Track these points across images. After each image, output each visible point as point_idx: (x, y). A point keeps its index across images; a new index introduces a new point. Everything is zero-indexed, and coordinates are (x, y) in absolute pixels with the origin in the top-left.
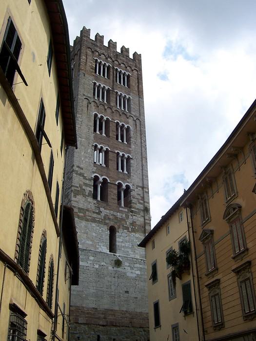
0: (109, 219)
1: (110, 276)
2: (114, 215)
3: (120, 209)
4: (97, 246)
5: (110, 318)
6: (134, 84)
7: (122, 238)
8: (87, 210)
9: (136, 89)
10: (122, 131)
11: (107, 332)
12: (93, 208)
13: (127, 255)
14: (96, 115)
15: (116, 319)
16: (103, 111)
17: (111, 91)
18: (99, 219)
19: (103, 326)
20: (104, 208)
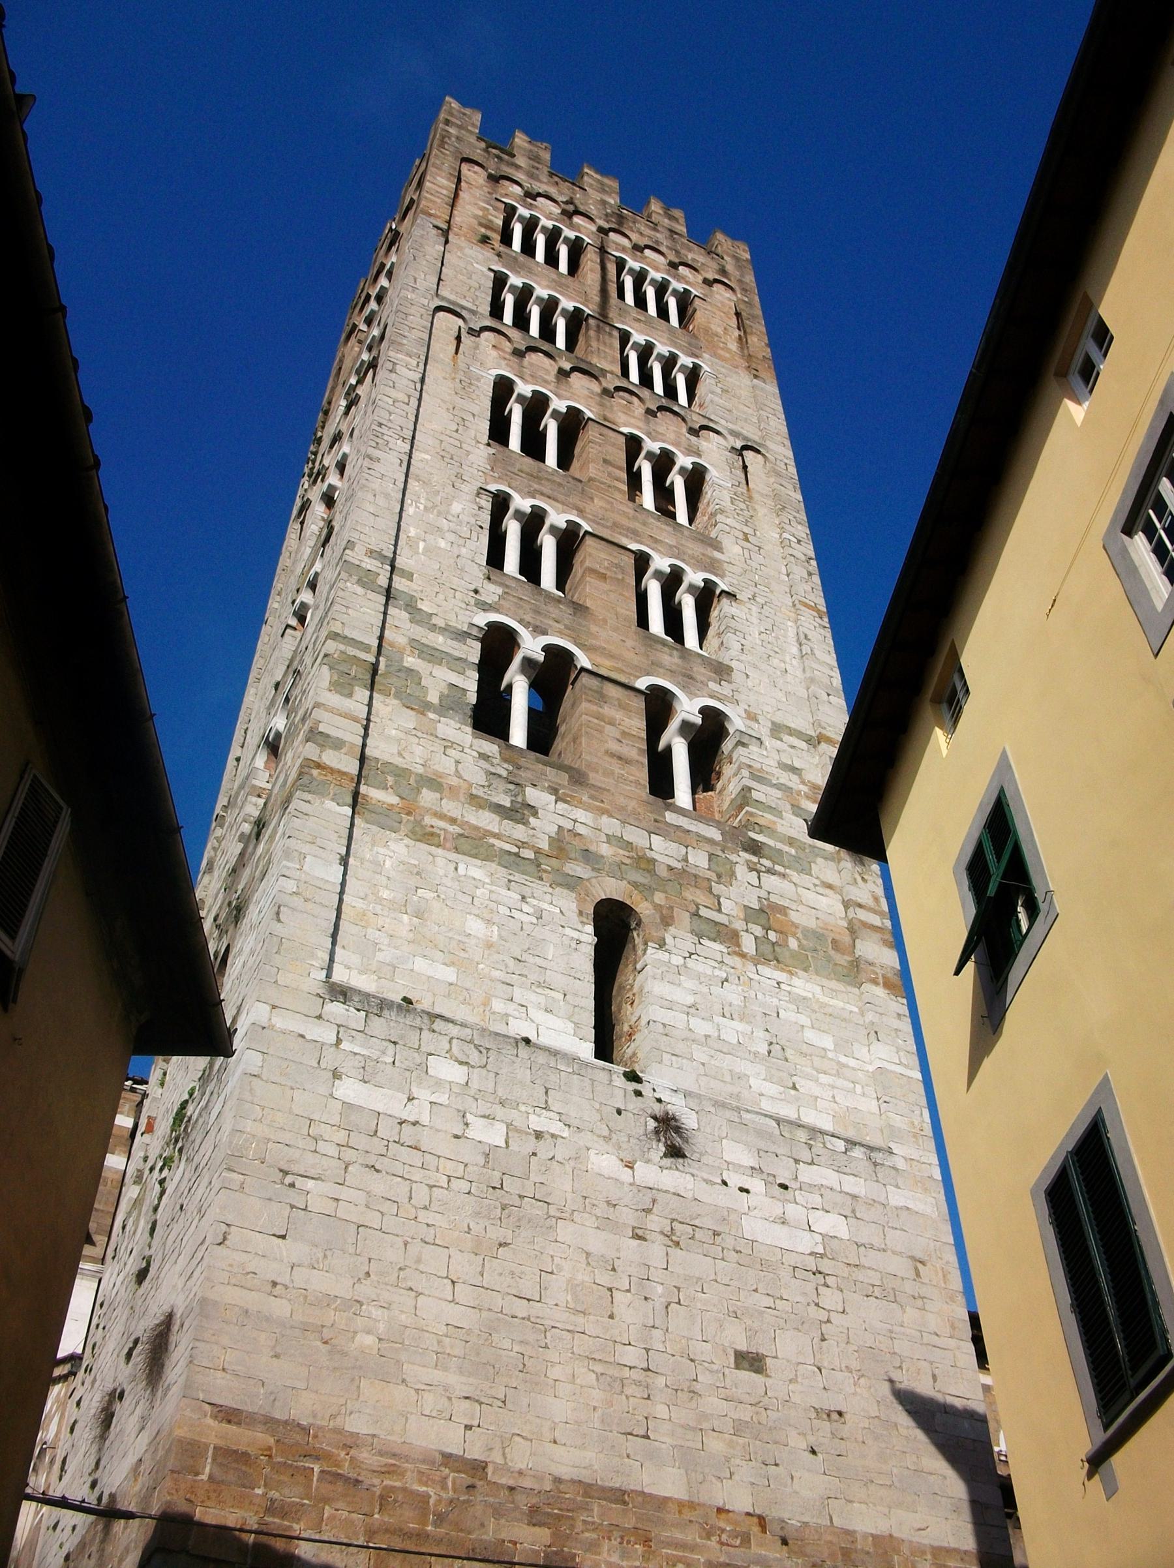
1: (606, 1224)
2: (629, 846)
3: (670, 817)
4: (498, 1006)
8: (433, 782)
12: (474, 774)
18: (522, 845)
20: (554, 791)
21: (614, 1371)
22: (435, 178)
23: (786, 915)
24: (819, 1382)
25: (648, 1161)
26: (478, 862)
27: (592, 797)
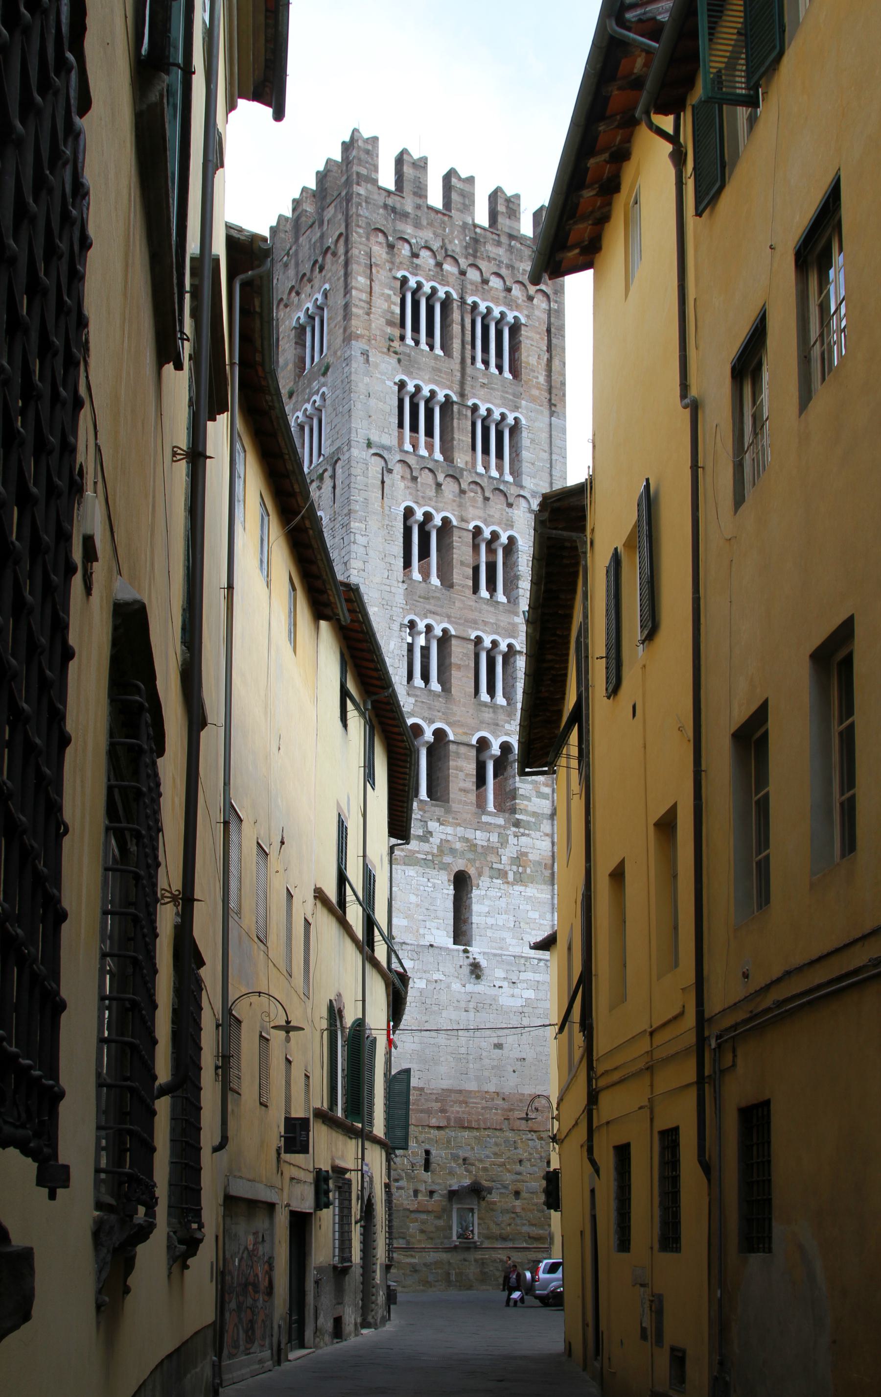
0: (453, 851)
1: (456, 1008)
2: (467, 840)
3: (485, 818)
4: (422, 931)
5: (456, 1110)
6: (533, 360)
7: (487, 902)
9: (542, 379)
10: (491, 551)
11: (449, 1142)
13: (501, 948)
14: (409, 512)
15: (469, 1114)
16: (432, 493)
17: (456, 407)
18: (427, 853)
19: (439, 1128)
20: (438, 820)
21: (459, 1056)
22: (357, 279)
23: (527, 856)
24: (519, 1049)
25: (470, 983)
26: (412, 867)
27: (453, 818)
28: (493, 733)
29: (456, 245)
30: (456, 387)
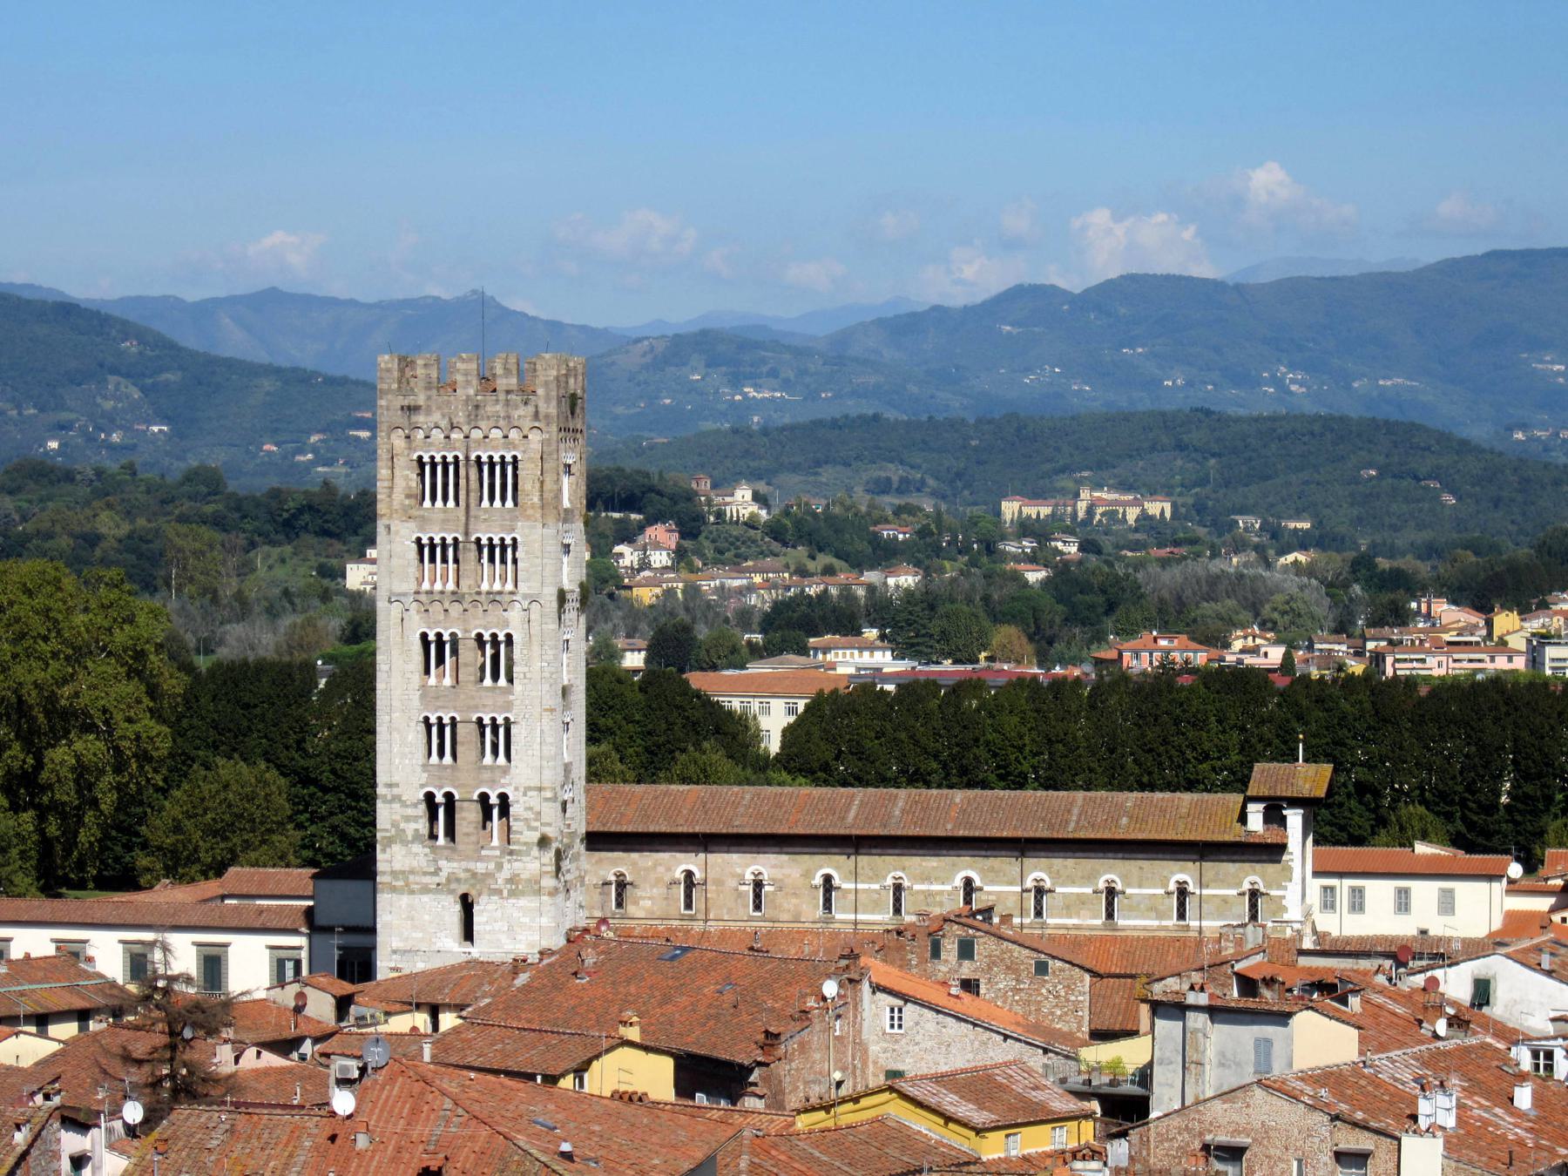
0: (458, 880)
3: (484, 853)
8: (412, 872)
12: (423, 862)
14: (424, 636)
16: (442, 617)
28: (491, 788)
29: (460, 418)
30: (462, 529)
